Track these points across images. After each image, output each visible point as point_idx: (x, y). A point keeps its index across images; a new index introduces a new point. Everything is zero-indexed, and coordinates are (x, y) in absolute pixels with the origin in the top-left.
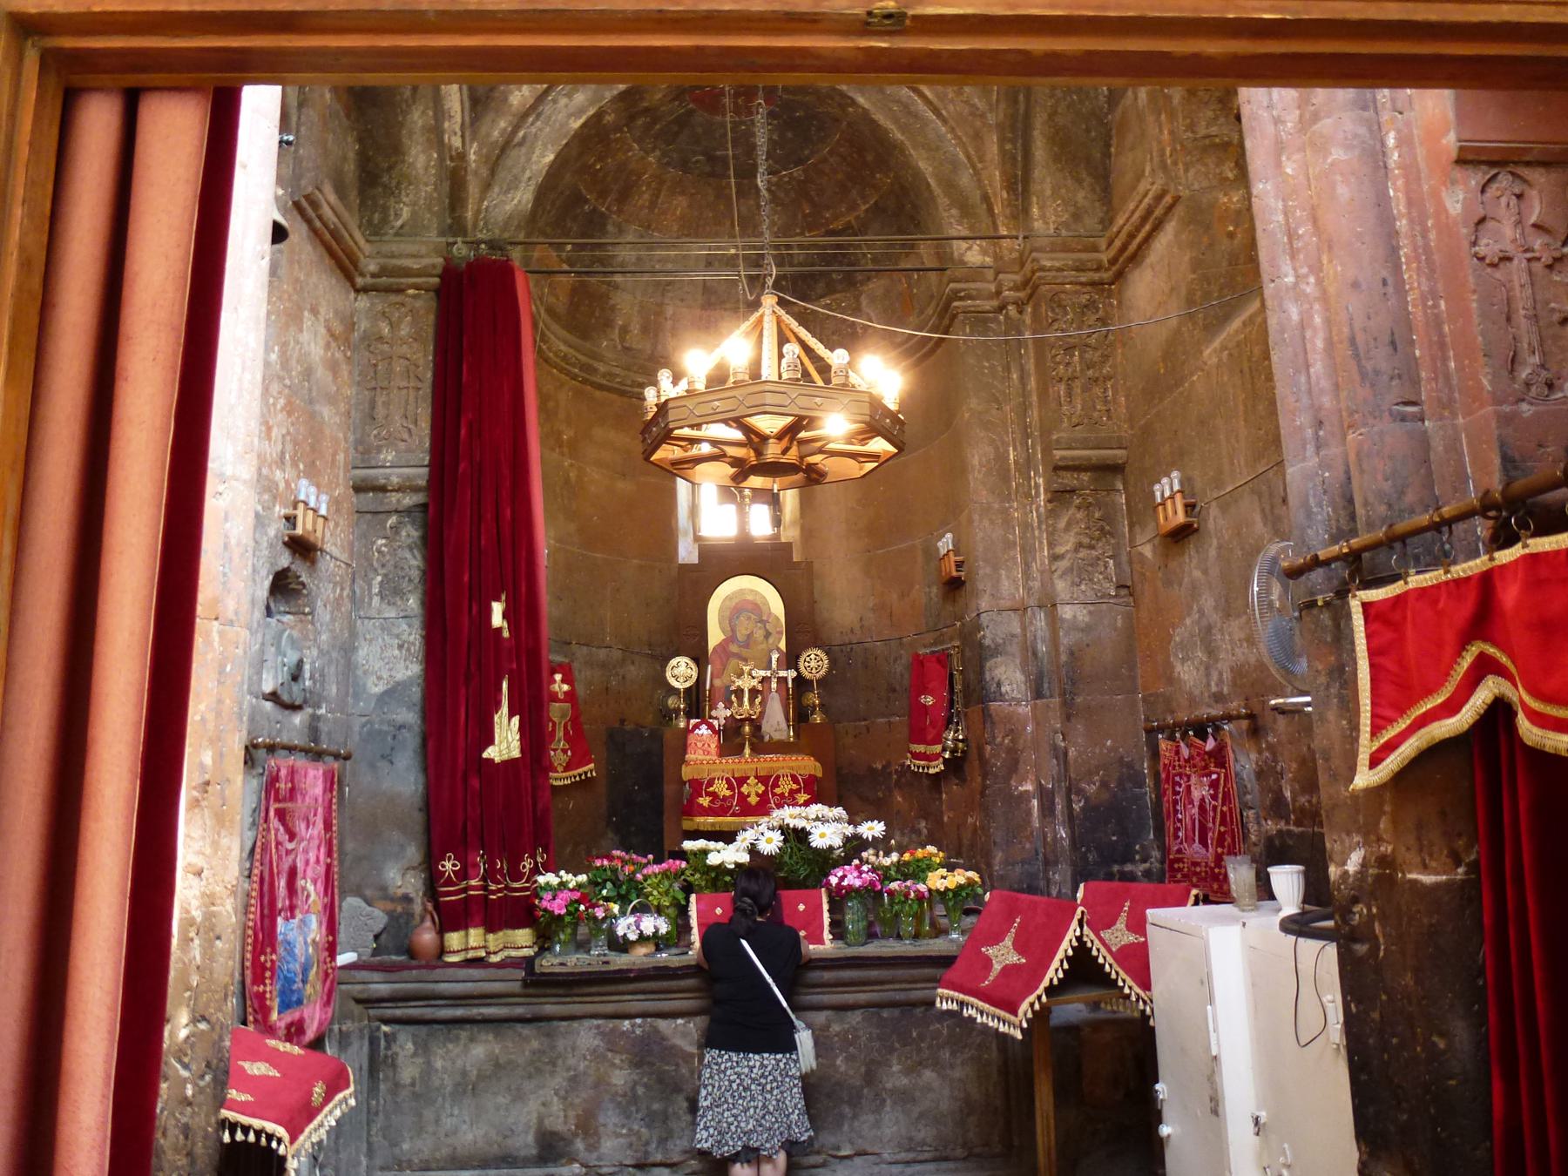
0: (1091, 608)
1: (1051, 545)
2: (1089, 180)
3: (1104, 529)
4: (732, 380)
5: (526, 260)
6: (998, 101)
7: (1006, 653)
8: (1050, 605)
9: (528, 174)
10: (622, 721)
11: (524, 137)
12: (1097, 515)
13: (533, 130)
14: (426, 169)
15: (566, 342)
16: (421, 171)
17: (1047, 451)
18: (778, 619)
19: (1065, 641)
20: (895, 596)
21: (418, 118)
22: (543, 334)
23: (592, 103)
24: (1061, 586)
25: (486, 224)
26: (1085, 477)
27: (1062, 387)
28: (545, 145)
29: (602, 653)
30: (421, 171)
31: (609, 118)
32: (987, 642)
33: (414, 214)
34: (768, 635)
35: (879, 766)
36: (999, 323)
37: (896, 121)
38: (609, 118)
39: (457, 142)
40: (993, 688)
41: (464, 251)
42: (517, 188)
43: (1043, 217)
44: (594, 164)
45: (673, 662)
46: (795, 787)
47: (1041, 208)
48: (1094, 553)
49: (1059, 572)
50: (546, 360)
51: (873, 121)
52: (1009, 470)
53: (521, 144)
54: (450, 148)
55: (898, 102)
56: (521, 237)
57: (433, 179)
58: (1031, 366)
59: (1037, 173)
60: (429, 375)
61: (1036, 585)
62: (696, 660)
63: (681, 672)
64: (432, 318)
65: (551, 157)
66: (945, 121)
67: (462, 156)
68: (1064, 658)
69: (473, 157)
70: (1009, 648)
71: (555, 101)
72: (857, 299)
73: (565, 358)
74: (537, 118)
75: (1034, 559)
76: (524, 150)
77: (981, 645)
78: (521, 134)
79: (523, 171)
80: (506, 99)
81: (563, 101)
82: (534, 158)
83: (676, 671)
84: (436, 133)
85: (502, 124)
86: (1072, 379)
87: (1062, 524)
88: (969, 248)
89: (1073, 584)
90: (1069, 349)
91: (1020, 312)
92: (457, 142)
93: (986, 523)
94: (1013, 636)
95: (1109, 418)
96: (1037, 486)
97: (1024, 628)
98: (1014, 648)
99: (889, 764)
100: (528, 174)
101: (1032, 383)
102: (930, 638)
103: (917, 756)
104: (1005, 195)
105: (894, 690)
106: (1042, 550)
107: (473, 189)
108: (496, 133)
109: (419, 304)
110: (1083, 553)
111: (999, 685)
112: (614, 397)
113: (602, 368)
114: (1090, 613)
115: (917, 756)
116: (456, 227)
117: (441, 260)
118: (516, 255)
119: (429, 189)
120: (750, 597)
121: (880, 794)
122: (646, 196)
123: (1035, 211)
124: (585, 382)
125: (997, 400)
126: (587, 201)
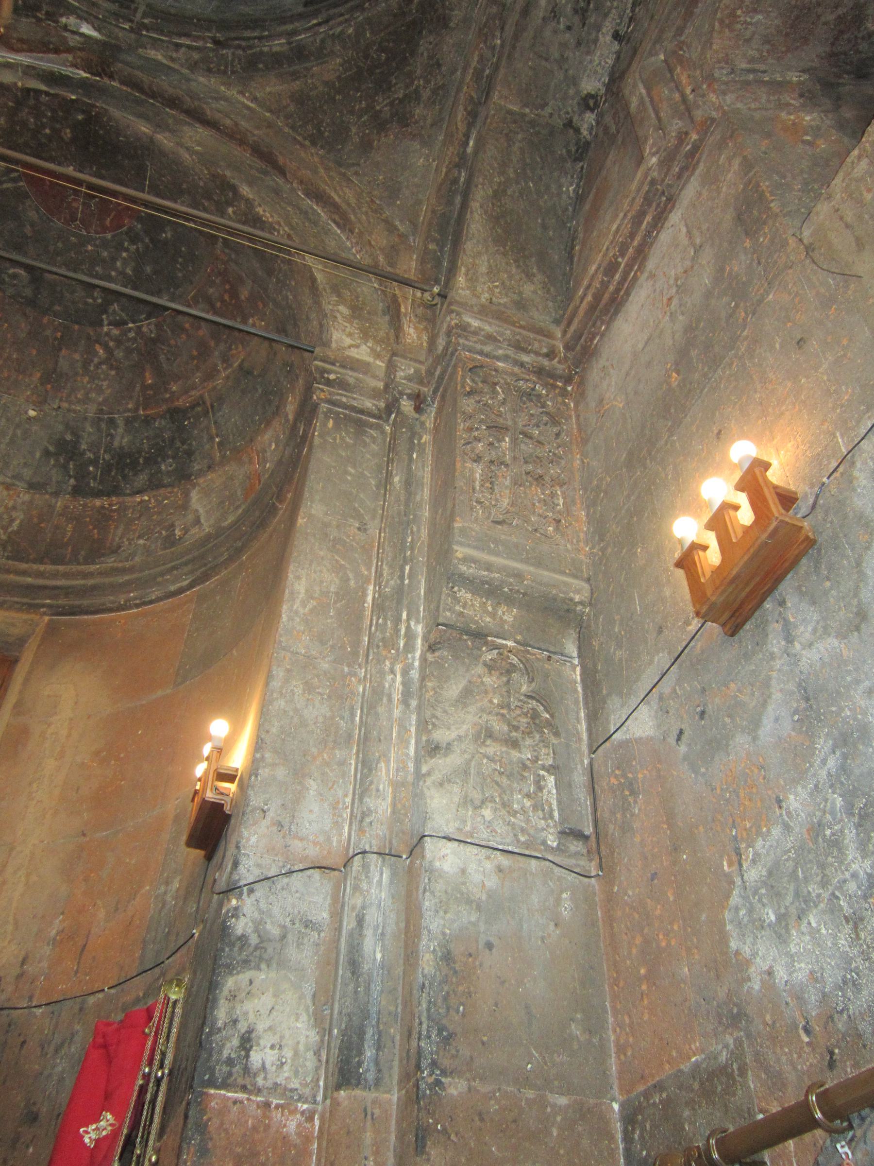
0: (505, 861)
1: (424, 726)
2: (539, 277)
3: (539, 715)
7: (282, 964)
8: (407, 850)
12: (524, 688)
19: (435, 924)
20: (102, 914)
24: (442, 808)
26: (509, 615)
27: (478, 471)
32: (240, 926)
36: (383, 432)
40: (230, 1047)
48: (515, 754)
49: (437, 776)
52: (360, 617)
59: (469, 246)
61: (381, 806)
68: (427, 963)
70: (292, 953)
72: (187, 495)
75: (385, 756)
77: (224, 930)
87: (454, 690)
88: (357, 346)
89: (466, 801)
91: (418, 409)
93: (297, 687)
94: (308, 924)
95: (557, 529)
96: (410, 636)
97: (337, 914)
98: (304, 956)
105: (33, 1118)
106: (404, 742)
110: (493, 748)
111: (247, 1042)
114: (500, 869)
123: (461, 280)
125: (359, 517)
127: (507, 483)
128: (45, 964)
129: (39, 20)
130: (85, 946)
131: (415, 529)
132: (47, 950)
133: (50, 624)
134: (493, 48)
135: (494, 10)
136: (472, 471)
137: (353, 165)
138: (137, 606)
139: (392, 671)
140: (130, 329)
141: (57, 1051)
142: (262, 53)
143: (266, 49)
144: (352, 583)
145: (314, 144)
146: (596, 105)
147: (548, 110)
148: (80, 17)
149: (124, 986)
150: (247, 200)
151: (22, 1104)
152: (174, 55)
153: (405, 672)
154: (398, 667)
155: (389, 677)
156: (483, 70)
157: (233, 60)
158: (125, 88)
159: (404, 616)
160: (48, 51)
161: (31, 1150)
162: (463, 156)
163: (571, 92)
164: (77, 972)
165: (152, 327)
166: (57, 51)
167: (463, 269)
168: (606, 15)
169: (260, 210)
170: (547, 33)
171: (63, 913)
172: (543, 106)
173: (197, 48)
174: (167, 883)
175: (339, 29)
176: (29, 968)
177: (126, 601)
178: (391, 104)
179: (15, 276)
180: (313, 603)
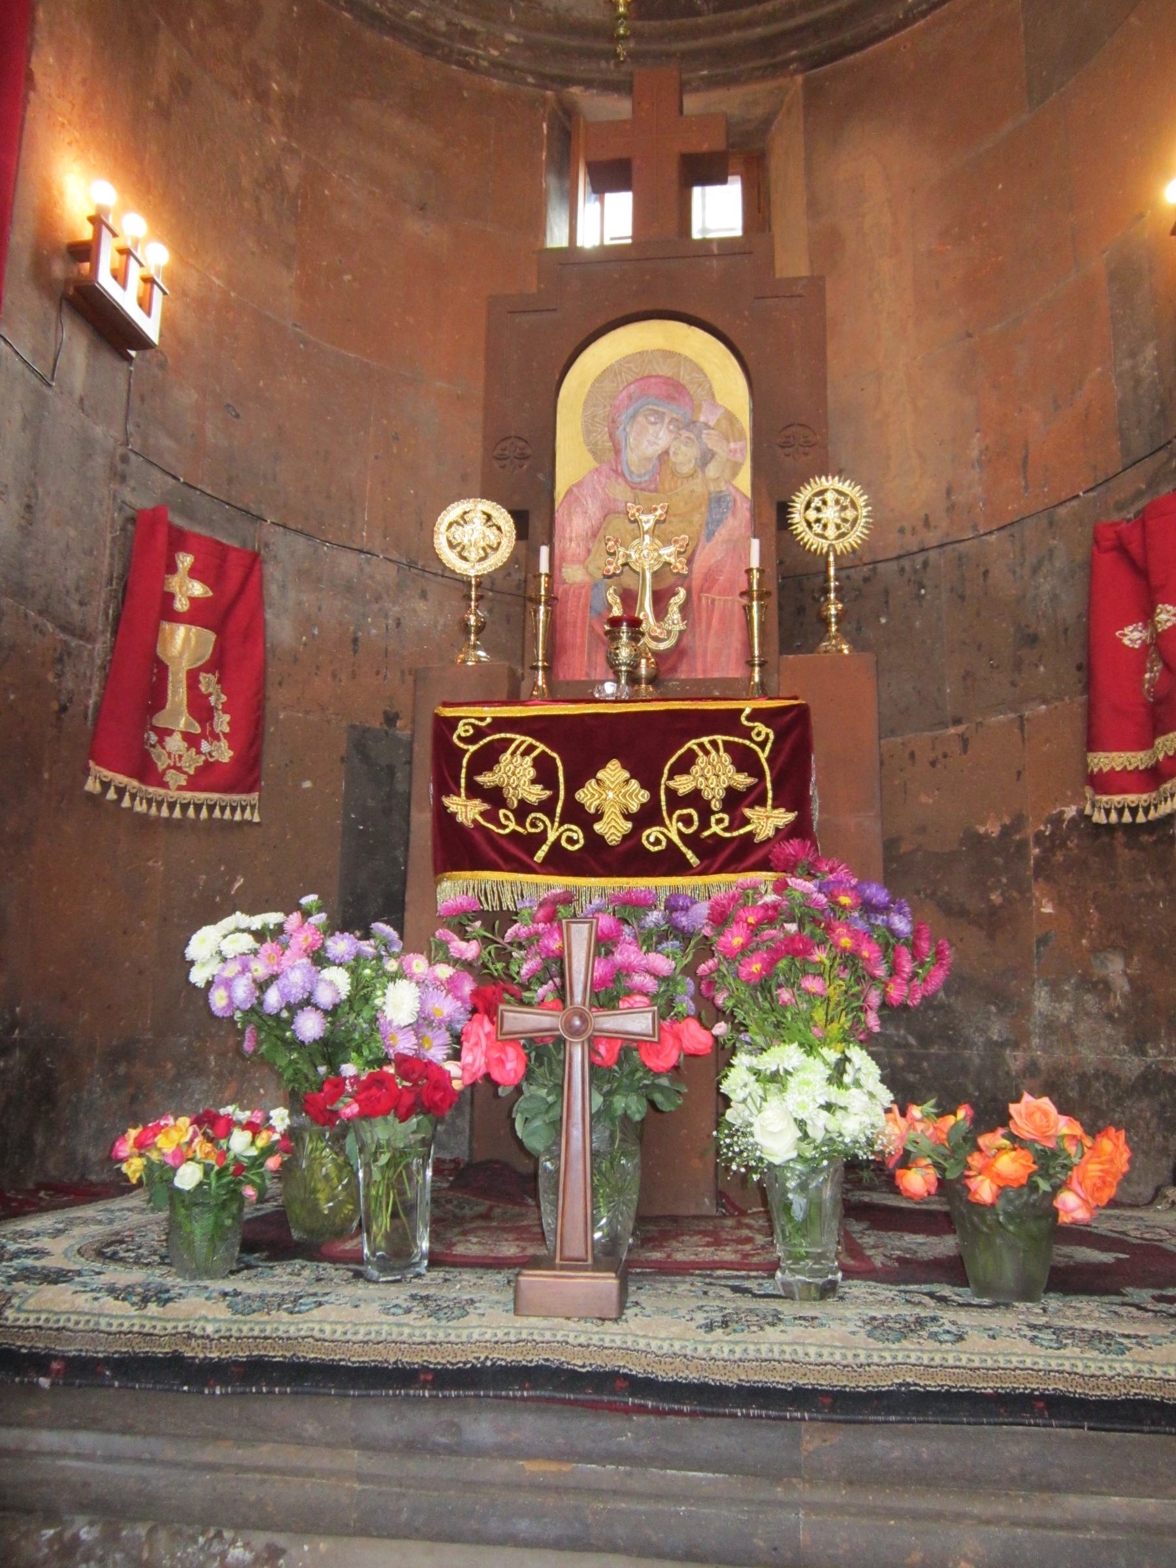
10: (391, 719)
18: (730, 418)
20: (1037, 417)
29: (347, 563)
34: (706, 457)
35: (992, 829)
45: (454, 512)
46: (743, 781)
62: (521, 519)
63: (473, 535)
83: (459, 534)
99: (1019, 821)
102: (1135, 480)
103: (1102, 783)
105: (1032, 640)
112: (410, 52)
115: (1102, 783)
120: (665, 370)
121: (995, 897)
128: (978, 489)
130: (1026, 457)
132: (975, 473)
133: (807, 82)
138: (923, 14)
141: (1035, 570)
149: (1112, 484)
151: (1012, 630)
161: (1042, 669)
164: (1026, 488)
171: (978, 431)
174: (1133, 354)
176: (958, 497)
177: (906, 13)
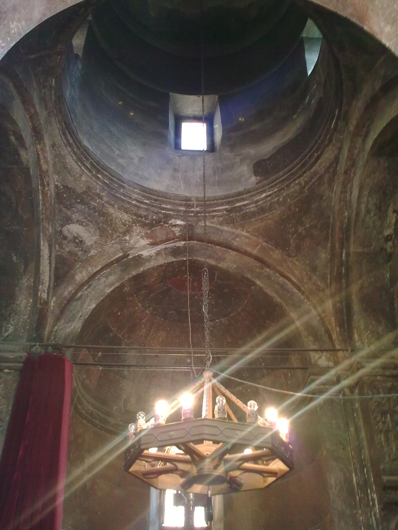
4: (183, 418)
5: (75, 356)
6: (331, 284)
9: (80, 314)
11: (81, 296)
13: (86, 292)
14: (26, 307)
15: (93, 405)
16: (23, 308)
17: (377, 476)
21: (26, 282)
22: (79, 399)
23: (117, 281)
25: (55, 338)
28: (91, 300)
30: (23, 308)
31: (126, 289)
33: (15, 330)
37: (277, 292)
38: (126, 289)
39: (45, 296)
41: (39, 350)
42: (74, 321)
43: (361, 339)
44: (117, 312)
47: (360, 335)
50: (81, 414)
51: (266, 294)
52: (353, 489)
53: (78, 299)
54: (41, 299)
55: (278, 284)
56: (73, 344)
57: (28, 312)
58: (361, 423)
59: (355, 317)
60: (8, 418)
64: (15, 385)
65: (94, 306)
66: (303, 293)
67: (46, 303)
69: (52, 304)
71: (99, 279)
73: (91, 414)
74: (89, 287)
76: (79, 302)
78: (79, 294)
79: (79, 311)
80: (73, 277)
81: (103, 279)
82: (85, 306)
84: (34, 290)
85: (70, 289)
86: (387, 431)
88: (320, 358)
90: (384, 414)
92: (45, 296)
96: (373, 500)
100: (80, 314)
101: (363, 434)
104: (338, 330)
107: (50, 320)
108: (66, 293)
109: (10, 377)
113: (112, 421)
116: (39, 338)
117: (26, 354)
118: (68, 354)
119: (25, 317)
122: (144, 331)
123: (356, 337)
124: (101, 428)
126: (111, 331)
127: (393, 438)
129: (162, 225)
131: (364, 452)
134: (345, 217)
135: (342, 203)
136: (381, 438)
137: (294, 256)
139: (371, 516)
140: (218, 322)
142: (246, 212)
143: (248, 210)
144: (347, 475)
145: (276, 248)
146: (391, 239)
147: (372, 248)
148: (175, 218)
150: (260, 287)
152: (213, 221)
153: (375, 515)
154: (373, 513)
155: (371, 520)
156: (343, 225)
157: (236, 218)
158: (198, 242)
159: (369, 490)
160: (171, 240)
162: (341, 261)
163: (381, 237)
165: (226, 321)
166: (173, 239)
167: (355, 331)
168: (389, 206)
169: (266, 291)
170: (367, 219)
172: (371, 246)
173: (221, 216)
175: (276, 199)
178: (305, 229)
179: (172, 314)
180: (338, 488)
